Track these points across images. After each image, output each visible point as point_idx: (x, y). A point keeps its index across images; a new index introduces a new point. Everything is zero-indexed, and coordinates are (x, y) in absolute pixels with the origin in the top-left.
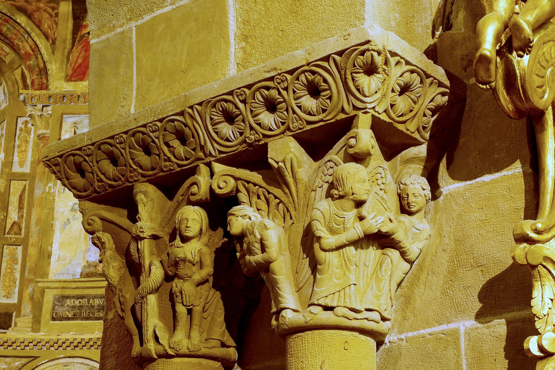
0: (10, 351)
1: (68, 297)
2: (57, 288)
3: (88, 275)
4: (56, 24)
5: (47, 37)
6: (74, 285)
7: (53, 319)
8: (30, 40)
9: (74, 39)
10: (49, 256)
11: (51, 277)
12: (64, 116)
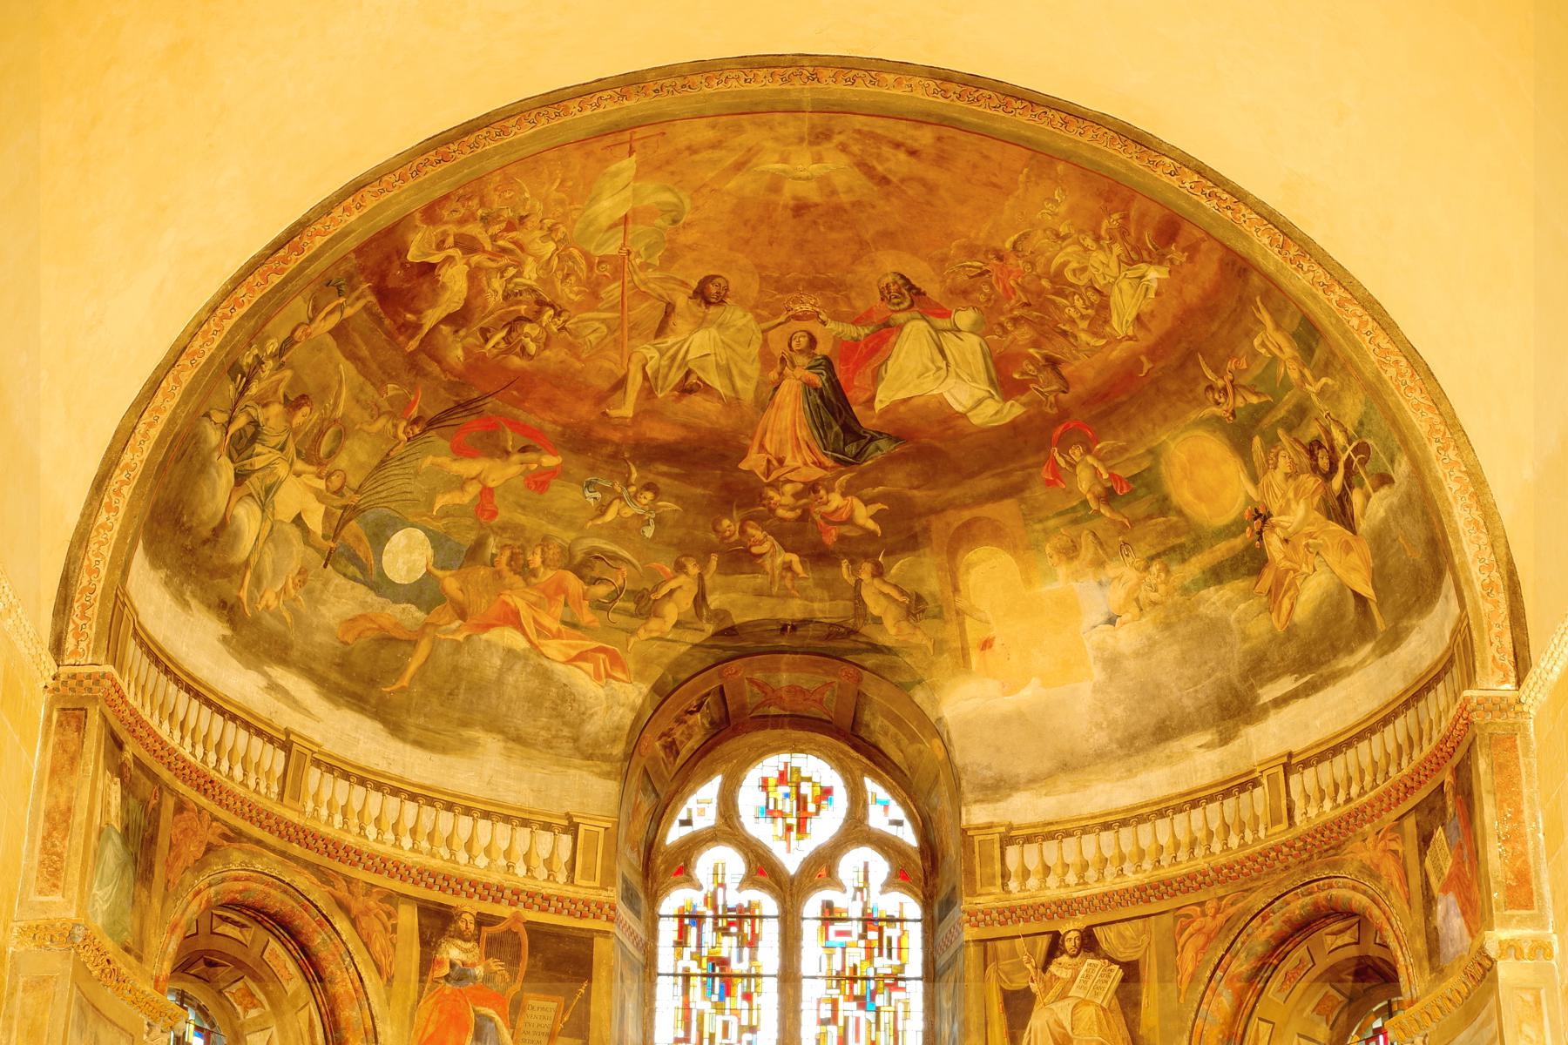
4: (394, 946)
8: (352, 969)
9: (421, 981)
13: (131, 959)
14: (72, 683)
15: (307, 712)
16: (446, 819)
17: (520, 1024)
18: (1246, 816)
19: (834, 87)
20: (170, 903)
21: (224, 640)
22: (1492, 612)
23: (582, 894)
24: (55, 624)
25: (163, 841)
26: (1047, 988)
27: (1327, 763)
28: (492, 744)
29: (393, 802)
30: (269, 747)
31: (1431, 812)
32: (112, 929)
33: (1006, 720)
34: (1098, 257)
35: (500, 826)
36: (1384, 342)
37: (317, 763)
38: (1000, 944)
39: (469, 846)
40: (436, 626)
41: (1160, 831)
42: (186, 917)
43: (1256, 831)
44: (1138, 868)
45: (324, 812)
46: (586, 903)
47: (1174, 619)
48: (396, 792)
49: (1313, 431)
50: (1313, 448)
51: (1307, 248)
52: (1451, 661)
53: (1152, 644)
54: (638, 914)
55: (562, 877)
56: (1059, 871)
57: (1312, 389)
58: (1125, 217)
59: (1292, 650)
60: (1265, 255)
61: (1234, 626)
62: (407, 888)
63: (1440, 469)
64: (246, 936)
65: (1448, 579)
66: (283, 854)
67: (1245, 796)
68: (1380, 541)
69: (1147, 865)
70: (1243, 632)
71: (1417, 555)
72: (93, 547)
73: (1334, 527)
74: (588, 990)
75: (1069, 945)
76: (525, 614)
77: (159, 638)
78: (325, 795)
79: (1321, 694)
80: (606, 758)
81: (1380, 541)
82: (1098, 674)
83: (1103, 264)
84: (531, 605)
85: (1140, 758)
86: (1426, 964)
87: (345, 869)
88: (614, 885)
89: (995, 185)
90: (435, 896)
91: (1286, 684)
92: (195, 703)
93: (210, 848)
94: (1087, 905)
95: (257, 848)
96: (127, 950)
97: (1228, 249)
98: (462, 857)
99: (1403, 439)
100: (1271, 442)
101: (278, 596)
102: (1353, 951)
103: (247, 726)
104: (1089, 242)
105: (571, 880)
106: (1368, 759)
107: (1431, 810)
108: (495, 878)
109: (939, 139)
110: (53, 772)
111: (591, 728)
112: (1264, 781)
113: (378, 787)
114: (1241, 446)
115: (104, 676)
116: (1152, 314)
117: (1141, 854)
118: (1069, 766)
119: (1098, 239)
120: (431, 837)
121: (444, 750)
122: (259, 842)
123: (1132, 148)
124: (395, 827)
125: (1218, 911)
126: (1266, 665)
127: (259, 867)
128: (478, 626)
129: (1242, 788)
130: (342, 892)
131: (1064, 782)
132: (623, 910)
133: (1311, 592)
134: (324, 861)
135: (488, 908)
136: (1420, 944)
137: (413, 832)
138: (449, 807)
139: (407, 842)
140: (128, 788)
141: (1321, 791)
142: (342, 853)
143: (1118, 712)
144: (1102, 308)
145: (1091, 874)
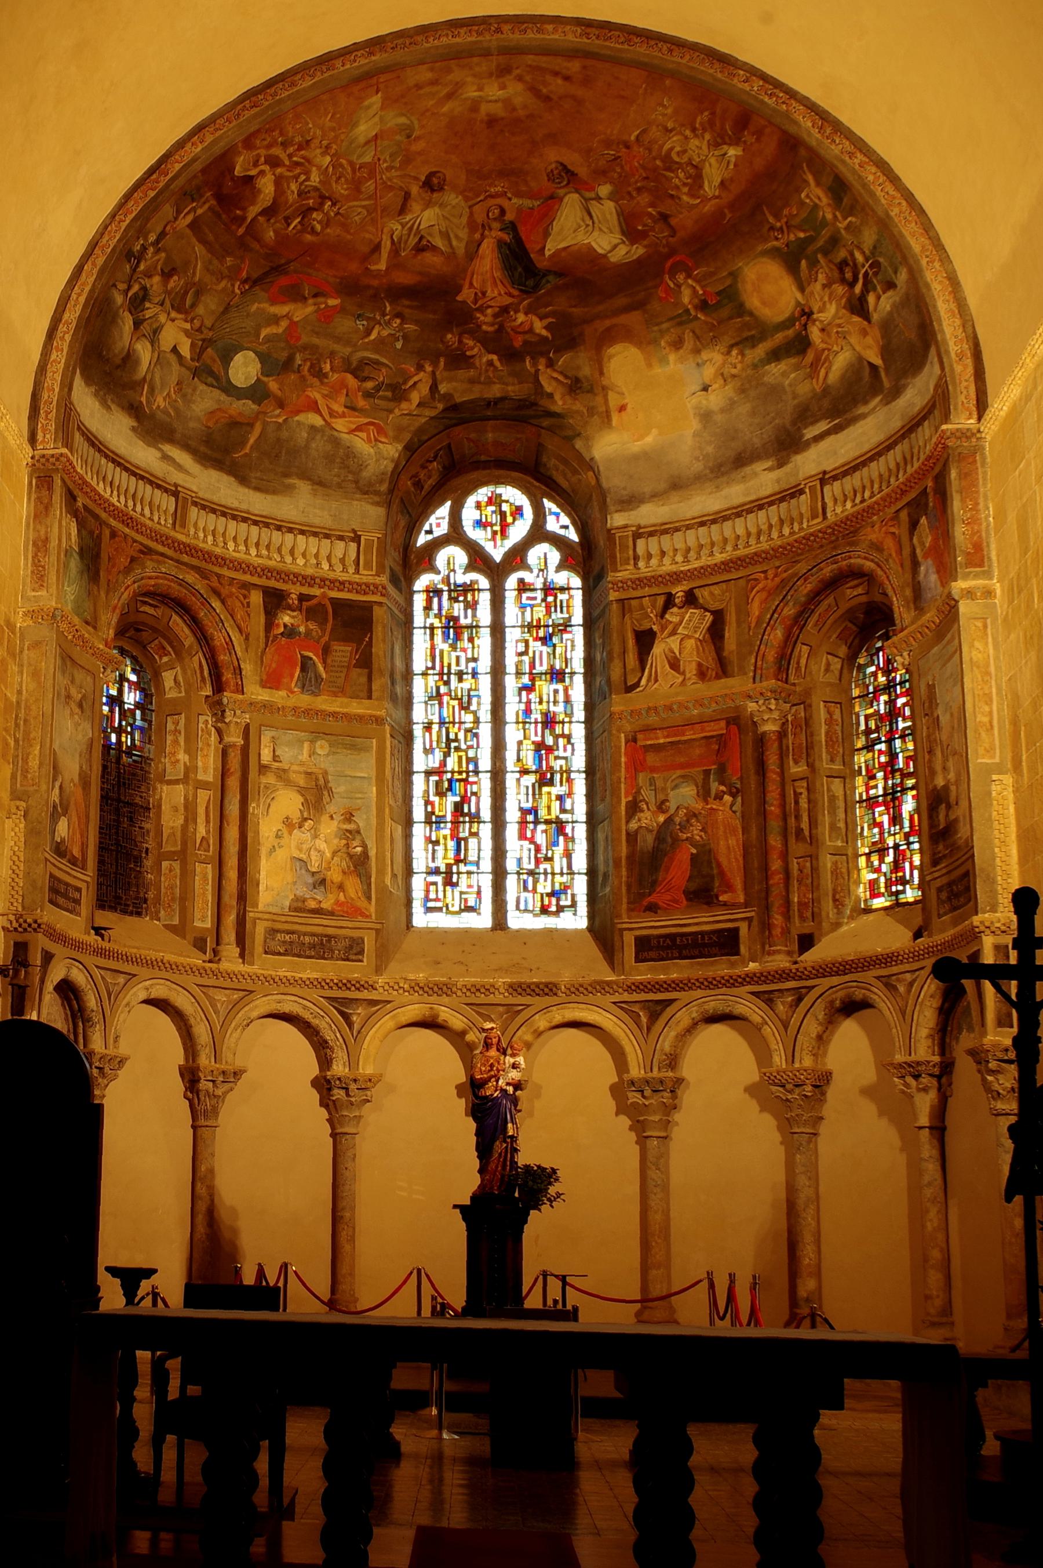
0: (228, 984)
1: (278, 931)
2: (268, 920)
3: (297, 910)
4: (249, 615)
5: (240, 631)
6: (283, 919)
7: (266, 953)
9: (267, 637)
10: (258, 885)
11: (261, 907)
12: (263, 728)
13: (90, 628)
14: (43, 460)
15: (187, 472)
16: (277, 536)
17: (329, 661)
18: (795, 514)
19: (513, 37)
20: (111, 594)
21: (134, 429)
22: (963, 371)
23: (365, 579)
24: (29, 425)
25: (104, 556)
26: (663, 628)
27: (849, 477)
28: (304, 488)
29: (244, 526)
30: (165, 494)
31: (917, 507)
32: (78, 610)
33: (636, 458)
34: (694, 143)
35: (311, 539)
36: (890, 189)
37: (195, 504)
38: (634, 603)
39: (292, 552)
40: (265, 413)
41: (739, 526)
42: (121, 602)
43: (801, 523)
44: (723, 550)
45: (201, 535)
46: (367, 585)
47: (747, 386)
48: (245, 520)
49: (842, 254)
50: (842, 266)
51: (838, 128)
52: (934, 406)
53: (731, 405)
54: (400, 591)
55: (351, 570)
56: (671, 554)
57: (841, 225)
58: (713, 114)
59: (826, 403)
60: (809, 134)
61: (787, 389)
62: (255, 580)
63: (929, 276)
64: (158, 613)
65: (933, 351)
66: (177, 561)
67: (794, 501)
68: (887, 326)
69: (729, 548)
70: (793, 392)
71: (912, 335)
72: (49, 374)
73: (856, 319)
74: (371, 638)
75: (677, 601)
76: (321, 403)
77: (94, 430)
78: (201, 524)
79: (845, 432)
80: (377, 493)
81: (887, 326)
82: (695, 424)
83: (698, 147)
84: (324, 396)
85: (725, 479)
86: (912, 605)
87: (216, 569)
88: (384, 573)
89: (623, 97)
90: (272, 583)
91: (823, 426)
92: (118, 469)
93: (133, 560)
94: (689, 575)
95: (161, 558)
96: (87, 623)
97: (785, 132)
98: (289, 559)
99: (902, 255)
100: (813, 264)
101: (165, 400)
102: (864, 599)
103: (151, 483)
104: (688, 133)
105: (357, 571)
106: (877, 473)
107: (918, 506)
108: (310, 571)
109: (584, 67)
110: (36, 516)
111: (365, 474)
112: (807, 490)
113: (234, 517)
114: (793, 269)
115: (62, 455)
116: (732, 180)
117: (725, 541)
118: (677, 485)
119: (694, 130)
120: (268, 547)
121: (274, 492)
122: (162, 555)
123: (717, 65)
124: (246, 541)
125: (776, 575)
126: (809, 413)
127: (164, 570)
128: (292, 412)
129: (793, 496)
130: (215, 584)
131: (675, 496)
132: (391, 589)
133: (840, 362)
134: (203, 564)
135: (305, 590)
136: (908, 592)
137: (257, 545)
138: (279, 528)
139: (253, 551)
140: (81, 525)
141: (845, 496)
142: (213, 559)
143: (710, 449)
144: (697, 177)
145: (692, 555)
